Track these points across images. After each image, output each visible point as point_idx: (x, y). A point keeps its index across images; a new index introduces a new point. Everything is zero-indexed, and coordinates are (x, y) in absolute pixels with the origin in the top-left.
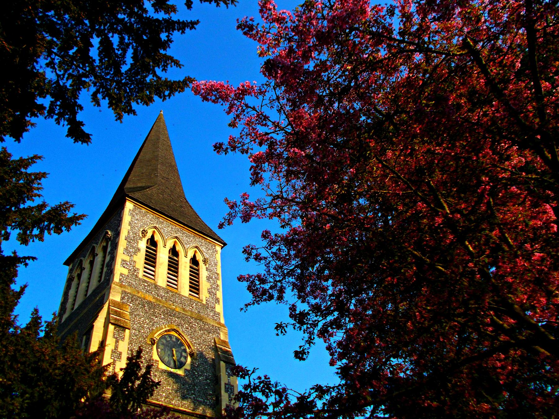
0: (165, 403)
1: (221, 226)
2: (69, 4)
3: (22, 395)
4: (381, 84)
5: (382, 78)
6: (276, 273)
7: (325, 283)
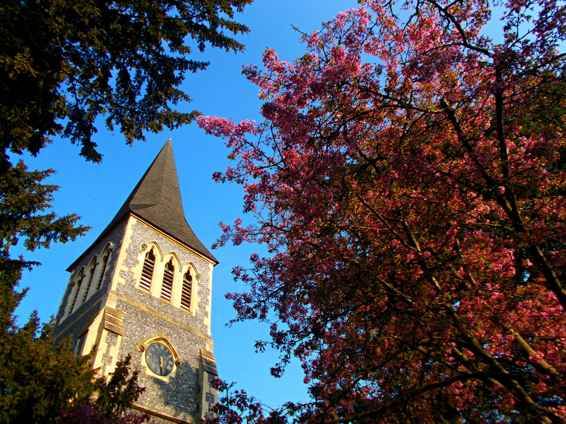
0: (149, 407)
1: (214, 247)
2: (93, 38)
3: (13, 392)
4: (367, 132)
5: (368, 126)
6: (261, 293)
7: (305, 306)
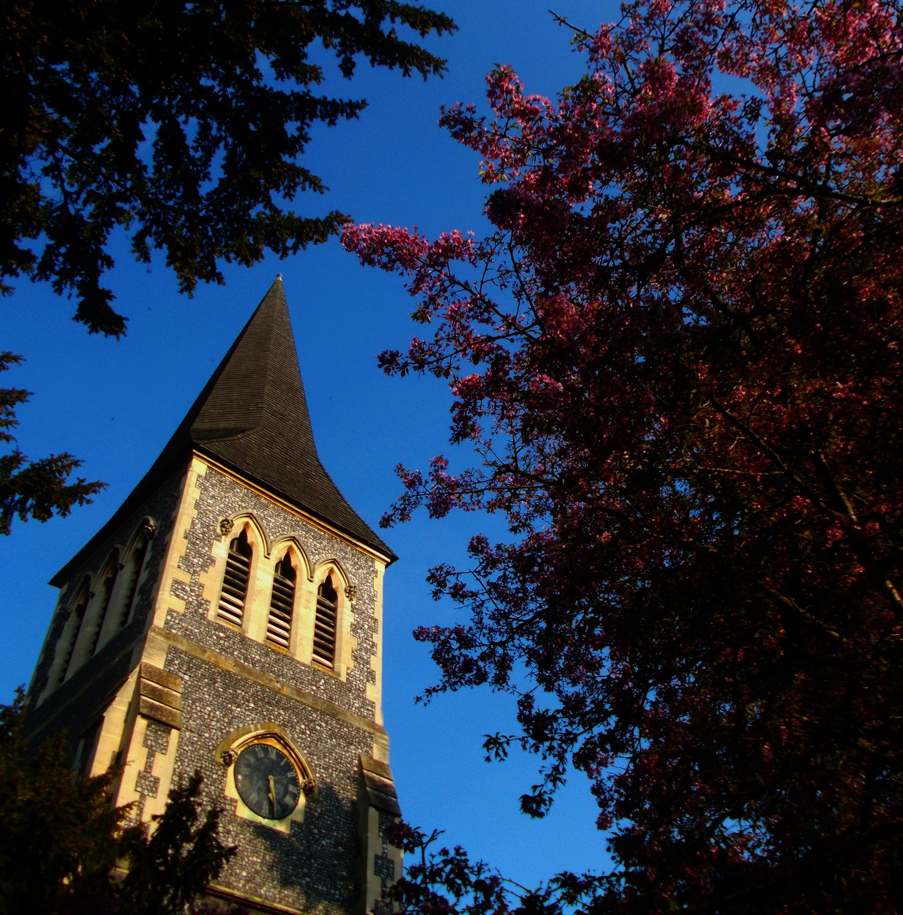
0: (246, 892)
1: (386, 522)
4: (728, 252)
5: (730, 239)
6: (495, 626)
7: (596, 653)
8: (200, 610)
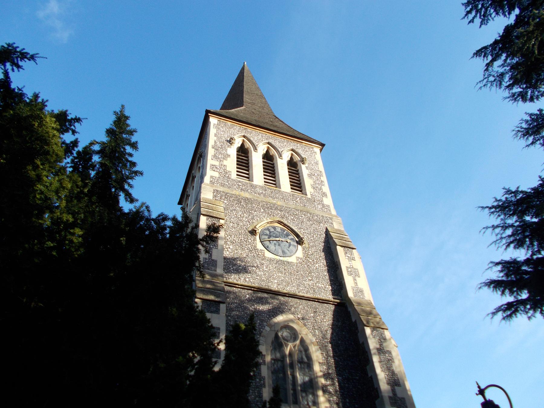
8: (227, 175)
